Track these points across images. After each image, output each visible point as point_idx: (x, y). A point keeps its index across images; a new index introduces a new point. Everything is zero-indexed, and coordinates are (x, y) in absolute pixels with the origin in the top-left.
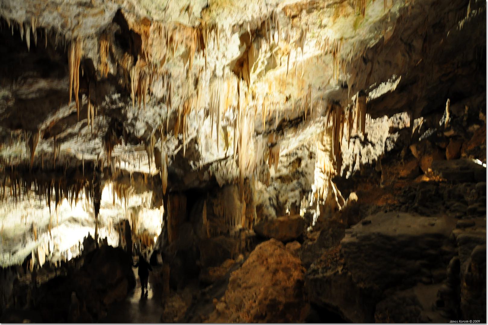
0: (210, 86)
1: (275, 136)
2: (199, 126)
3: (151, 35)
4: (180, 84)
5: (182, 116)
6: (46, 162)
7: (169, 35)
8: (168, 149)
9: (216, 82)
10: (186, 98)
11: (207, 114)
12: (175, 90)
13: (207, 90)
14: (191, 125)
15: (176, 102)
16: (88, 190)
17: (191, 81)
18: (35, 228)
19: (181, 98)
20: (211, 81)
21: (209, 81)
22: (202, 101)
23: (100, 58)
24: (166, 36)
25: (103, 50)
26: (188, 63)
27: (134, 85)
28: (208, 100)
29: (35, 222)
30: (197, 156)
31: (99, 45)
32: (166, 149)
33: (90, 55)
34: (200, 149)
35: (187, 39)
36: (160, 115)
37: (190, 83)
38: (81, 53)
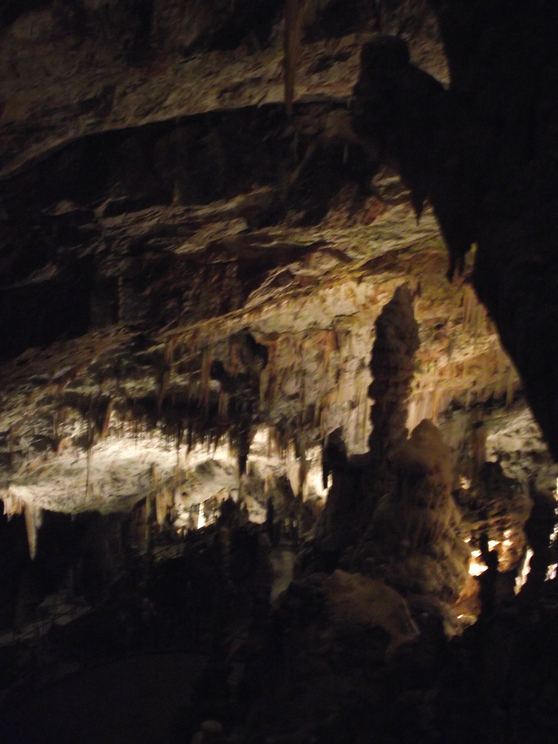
3: (279, 348)
5: (321, 409)
7: (299, 343)
13: (352, 382)
15: (311, 397)
16: (232, 436)
17: (331, 374)
18: (157, 470)
23: (230, 360)
24: (294, 345)
25: (234, 352)
27: (263, 387)
31: (231, 349)
33: (221, 359)
36: (294, 408)
38: (212, 358)
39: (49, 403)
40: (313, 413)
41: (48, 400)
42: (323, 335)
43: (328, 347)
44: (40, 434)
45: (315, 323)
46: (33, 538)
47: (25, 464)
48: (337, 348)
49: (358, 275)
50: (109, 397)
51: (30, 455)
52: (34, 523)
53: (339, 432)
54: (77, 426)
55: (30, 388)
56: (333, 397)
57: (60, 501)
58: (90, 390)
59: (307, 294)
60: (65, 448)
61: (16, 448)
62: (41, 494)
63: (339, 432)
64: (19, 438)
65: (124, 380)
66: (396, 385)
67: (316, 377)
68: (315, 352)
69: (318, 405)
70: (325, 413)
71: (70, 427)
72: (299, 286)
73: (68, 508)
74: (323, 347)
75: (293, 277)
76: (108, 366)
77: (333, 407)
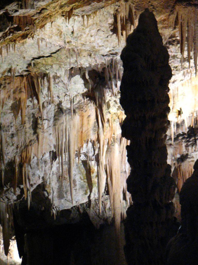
0: (54, 125)
1: (184, 145)
2: (45, 174)
4: (15, 132)
5: (21, 166)
8: (9, 199)
9: (64, 118)
10: (23, 147)
11: (54, 156)
12: (9, 140)
13: (51, 131)
14: (34, 174)
17: (28, 125)
19: (17, 147)
20: (56, 119)
21: (52, 120)
22: (48, 140)
26: (20, 115)
28: (54, 142)
30: (48, 204)
32: (6, 200)
34: (50, 197)
35: (14, 93)
37: (27, 129)
40: (13, 170)
42: (17, 83)
43: (24, 96)
45: (10, 70)
48: (34, 93)
49: (67, 9)
53: (42, 187)
56: (33, 151)
59: (24, 37)
63: (42, 187)
66: (153, 120)
67: (13, 130)
68: (10, 103)
69: (18, 160)
70: (27, 169)
72: (18, 29)
74: (18, 96)
75: (11, 19)
77: (34, 161)
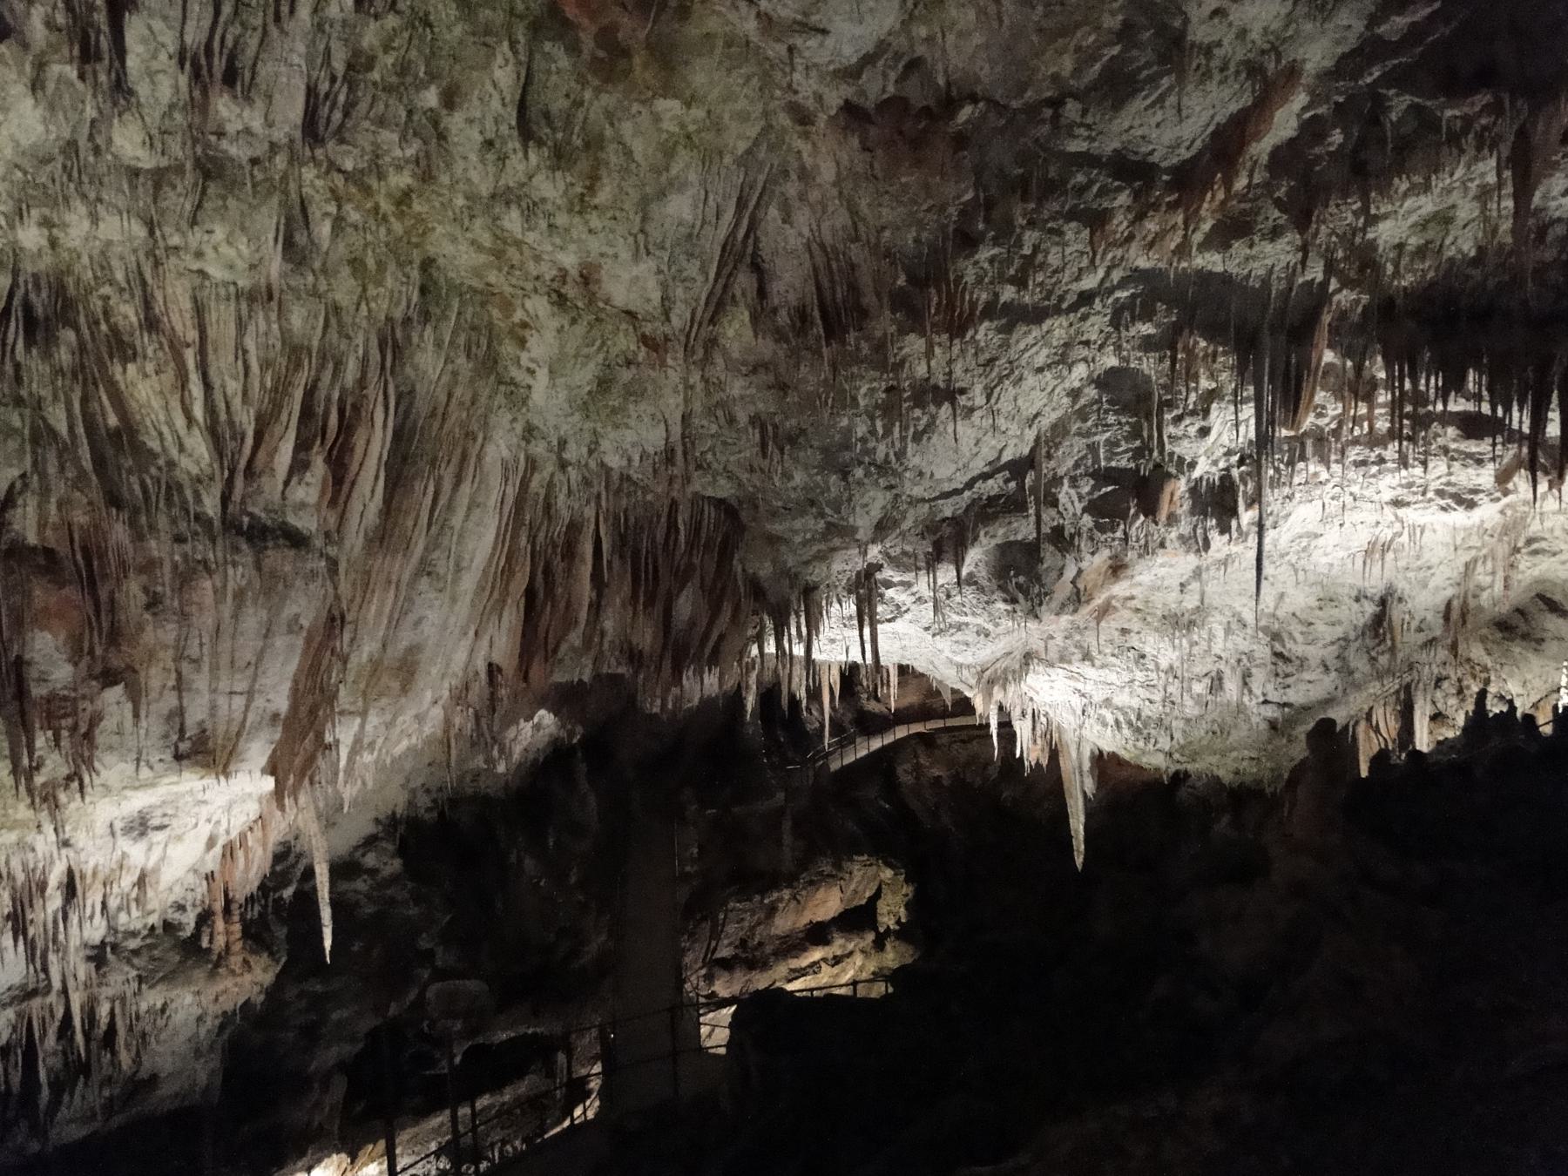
6: (1541, 270)
18: (1396, 613)
29: (1401, 585)
39: (1147, 315)
41: (1151, 291)
44: (1113, 464)
46: (1078, 824)
47: (1070, 573)
50: (1325, 284)
51: (1084, 545)
52: (1079, 788)
54: (1220, 416)
55: (1103, 192)
57: (1140, 726)
58: (1268, 258)
60: (1172, 519)
61: (1049, 517)
62: (1098, 697)
64: (1057, 481)
65: (1385, 190)
71: (1197, 426)
73: (1155, 757)
76: (1337, 137)
